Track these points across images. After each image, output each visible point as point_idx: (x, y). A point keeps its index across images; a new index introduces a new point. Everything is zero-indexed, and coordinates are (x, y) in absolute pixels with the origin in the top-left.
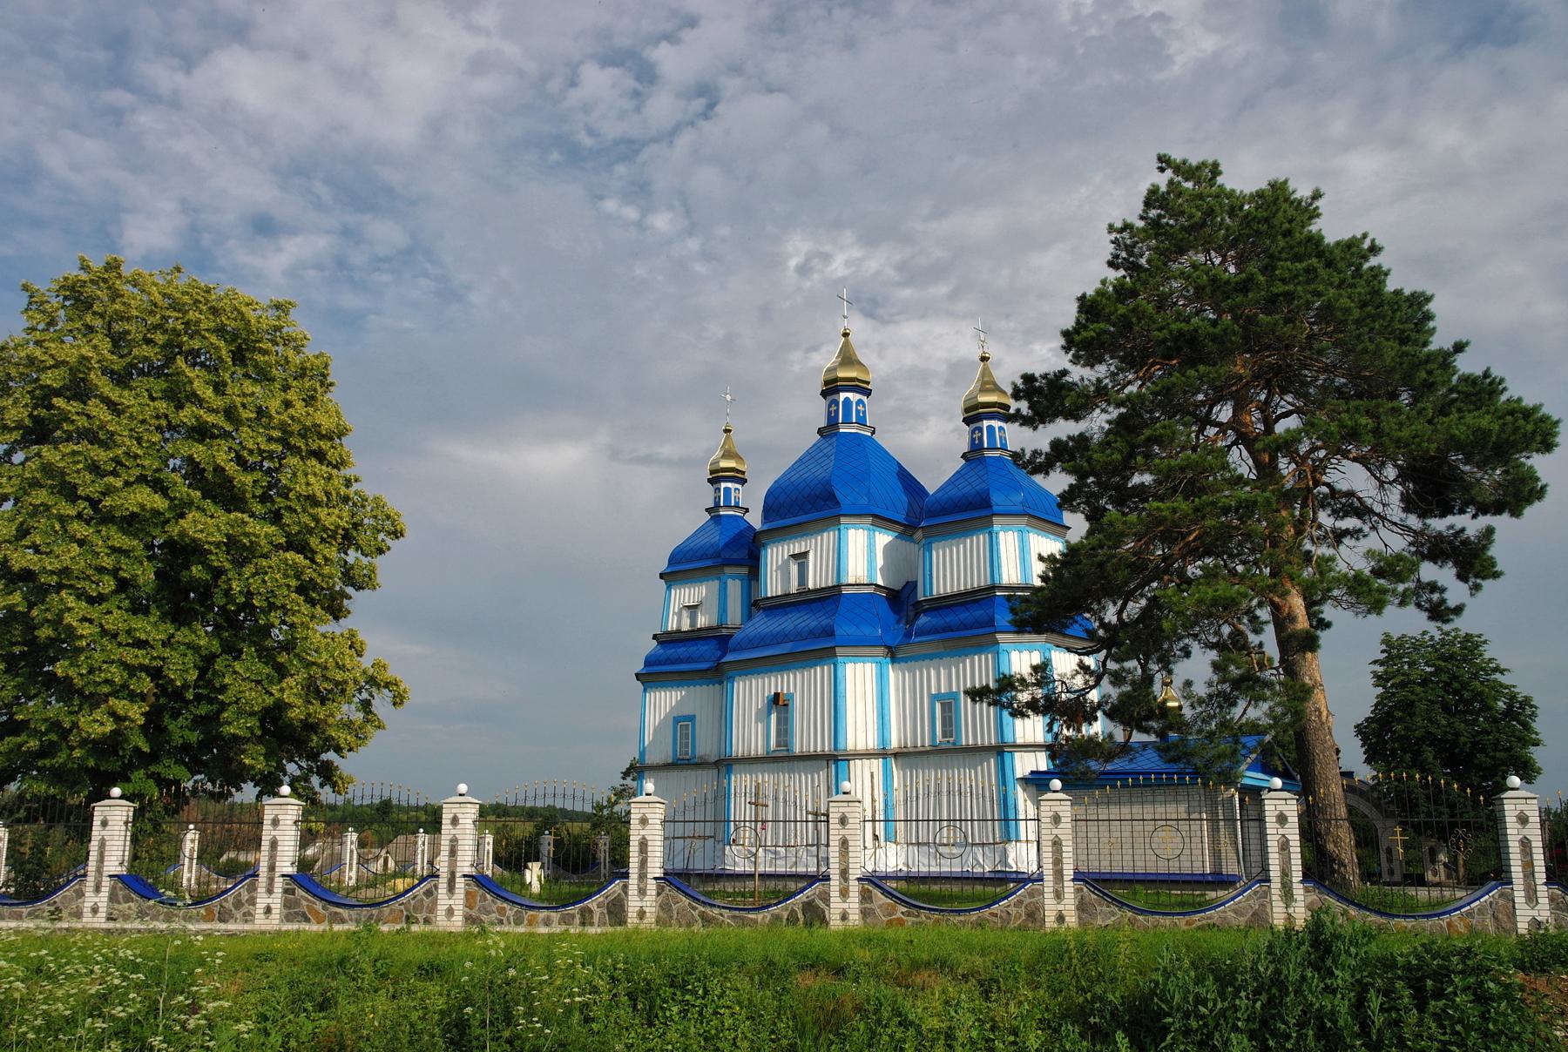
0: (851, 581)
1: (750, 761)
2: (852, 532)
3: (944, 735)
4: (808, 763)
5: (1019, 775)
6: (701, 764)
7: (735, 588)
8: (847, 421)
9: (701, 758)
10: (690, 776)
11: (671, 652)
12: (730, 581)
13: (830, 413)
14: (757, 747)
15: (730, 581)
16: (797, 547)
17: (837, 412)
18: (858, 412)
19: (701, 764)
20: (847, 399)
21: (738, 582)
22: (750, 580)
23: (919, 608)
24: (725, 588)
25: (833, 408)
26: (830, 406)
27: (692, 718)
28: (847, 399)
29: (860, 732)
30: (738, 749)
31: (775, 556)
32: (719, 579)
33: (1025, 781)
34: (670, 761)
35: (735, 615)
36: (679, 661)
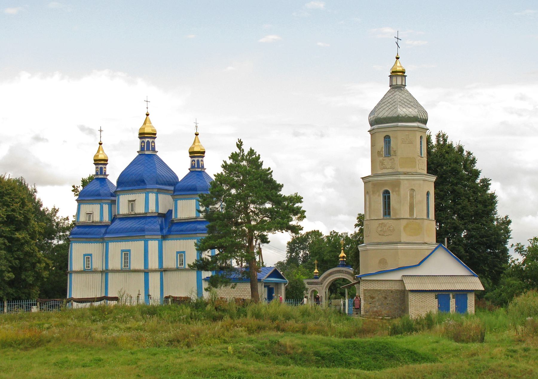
0: (150, 211)
1: (114, 271)
2: (150, 195)
3: (180, 265)
4: (135, 273)
5: (203, 278)
6: (95, 271)
7: (106, 207)
8: (148, 149)
9: (95, 269)
10: (90, 276)
11: (81, 230)
12: (104, 205)
13: (141, 146)
14: (118, 266)
15: (104, 205)
16: (131, 197)
17: (144, 146)
18: (152, 146)
19: (95, 271)
20: (148, 141)
21: (107, 206)
22: (111, 205)
23: (173, 223)
24: (103, 208)
25: (143, 144)
26: (142, 143)
27: (91, 255)
28: (148, 141)
29: (154, 264)
30: (110, 267)
31: (123, 200)
32: (100, 204)
33: (205, 280)
34: (83, 269)
35: (106, 219)
36: (85, 234)
